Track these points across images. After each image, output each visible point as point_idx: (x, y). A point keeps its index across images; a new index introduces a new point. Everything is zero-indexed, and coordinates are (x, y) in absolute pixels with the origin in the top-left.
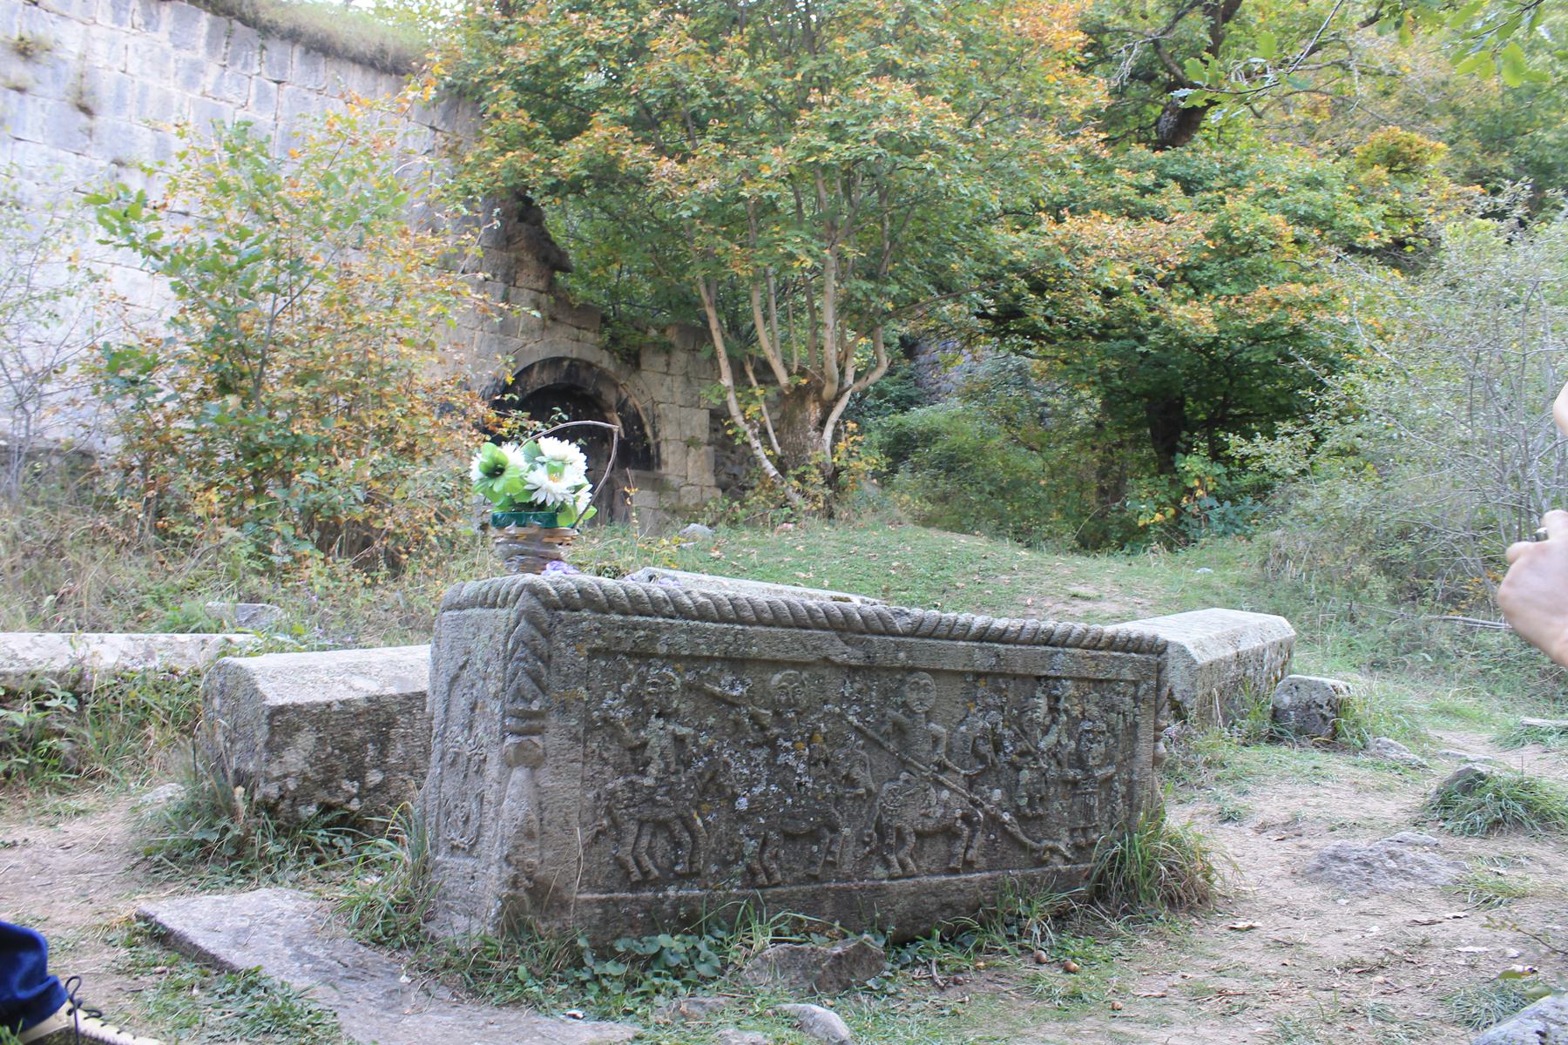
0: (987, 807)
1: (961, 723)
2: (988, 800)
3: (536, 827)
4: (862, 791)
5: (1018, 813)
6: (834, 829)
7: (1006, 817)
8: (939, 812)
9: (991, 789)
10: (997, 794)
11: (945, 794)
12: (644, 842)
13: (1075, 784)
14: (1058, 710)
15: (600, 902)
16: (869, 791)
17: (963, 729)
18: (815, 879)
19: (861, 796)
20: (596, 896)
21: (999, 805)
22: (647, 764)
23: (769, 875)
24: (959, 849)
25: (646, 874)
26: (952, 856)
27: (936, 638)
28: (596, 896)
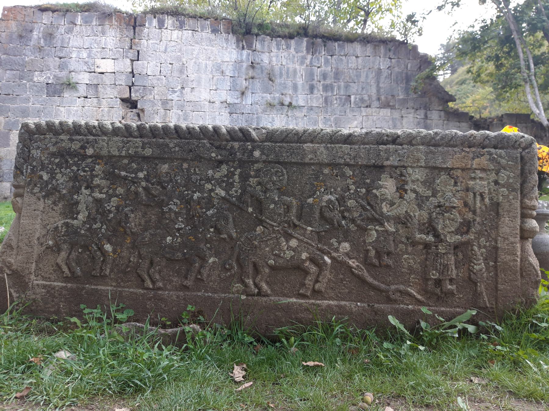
0: (335, 254)
1: (310, 197)
2: (337, 250)
3: (14, 244)
4: (224, 236)
5: (366, 262)
6: (204, 260)
7: (353, 263)
8: (289, 254)
9: (339, 243)
10: (346, 246)
11: (294, 243)
12: (74, 255)
13: (427, 246)
14: (406, 191)
15: (44, 287)
16: (230, 237)
17: (310, 200)
18: (186, 288)
19: (224, 239)
20: (44, 282)
21: (347, 254)
22: (78, 213)
23: (153, 282)
24: (309, 281)
25: (73, 273)
26: (303, 285)
27: (287, 142)
28: (44, 282)
